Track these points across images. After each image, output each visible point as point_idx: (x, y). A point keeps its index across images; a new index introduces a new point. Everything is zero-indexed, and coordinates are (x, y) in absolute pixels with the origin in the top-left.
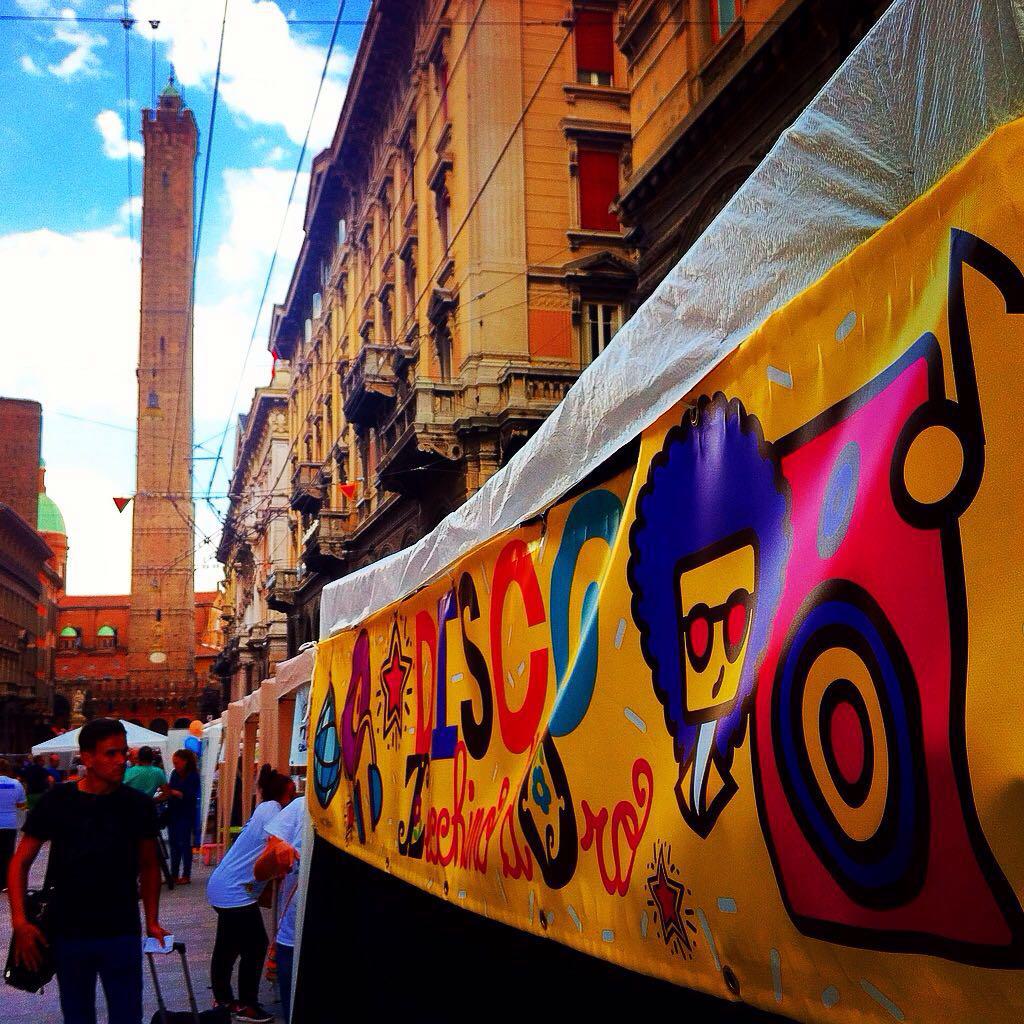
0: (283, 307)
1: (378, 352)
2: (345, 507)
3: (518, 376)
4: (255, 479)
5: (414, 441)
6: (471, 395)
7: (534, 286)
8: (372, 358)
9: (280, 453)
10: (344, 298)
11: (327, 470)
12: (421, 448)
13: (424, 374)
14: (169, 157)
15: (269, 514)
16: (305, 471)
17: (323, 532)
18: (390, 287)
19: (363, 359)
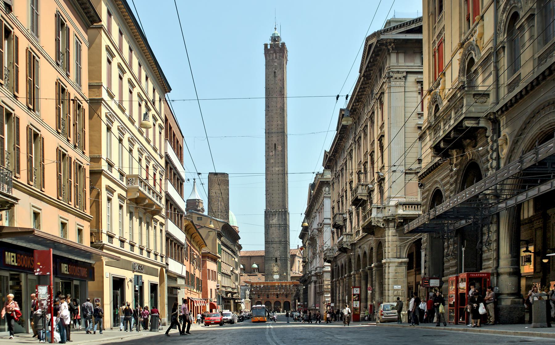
0: (329, 153)
1: (362, 185)
2: (351, 231)
3: (400, 204)
4: (317, 210)
5: (371, 222)
6: (387, 209)
7: (407, 175)
8: (360, 187)
9: (328, 204)
10: (351, 158)
11: (345, 216)
12: (373, 224)
13: (376, 196)
14: (276, 64)
15: (322, 224)
16: (338, 215)
17: (345, 240)
18: (367, 162)
19: (358, 187)
